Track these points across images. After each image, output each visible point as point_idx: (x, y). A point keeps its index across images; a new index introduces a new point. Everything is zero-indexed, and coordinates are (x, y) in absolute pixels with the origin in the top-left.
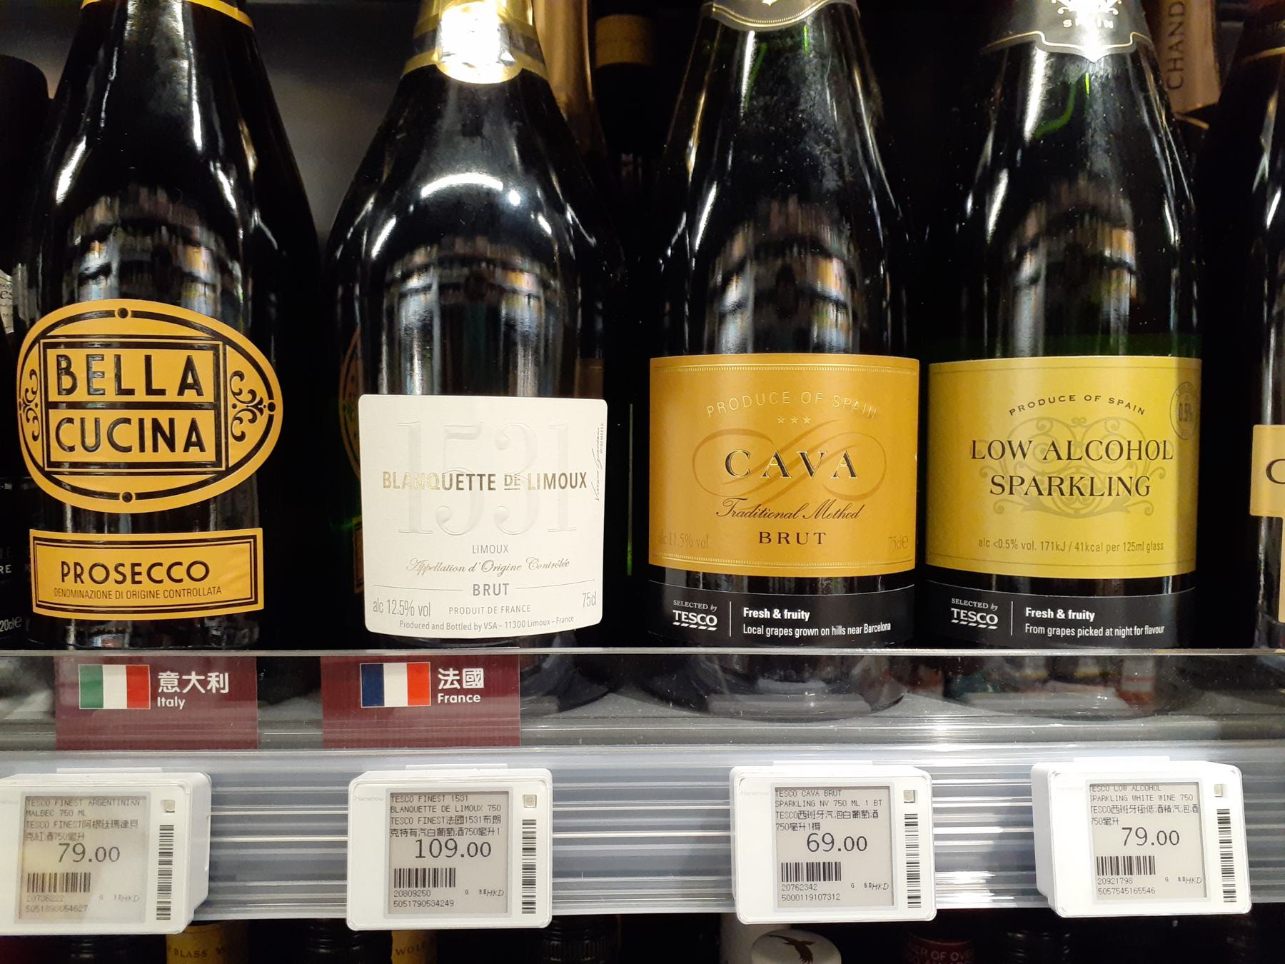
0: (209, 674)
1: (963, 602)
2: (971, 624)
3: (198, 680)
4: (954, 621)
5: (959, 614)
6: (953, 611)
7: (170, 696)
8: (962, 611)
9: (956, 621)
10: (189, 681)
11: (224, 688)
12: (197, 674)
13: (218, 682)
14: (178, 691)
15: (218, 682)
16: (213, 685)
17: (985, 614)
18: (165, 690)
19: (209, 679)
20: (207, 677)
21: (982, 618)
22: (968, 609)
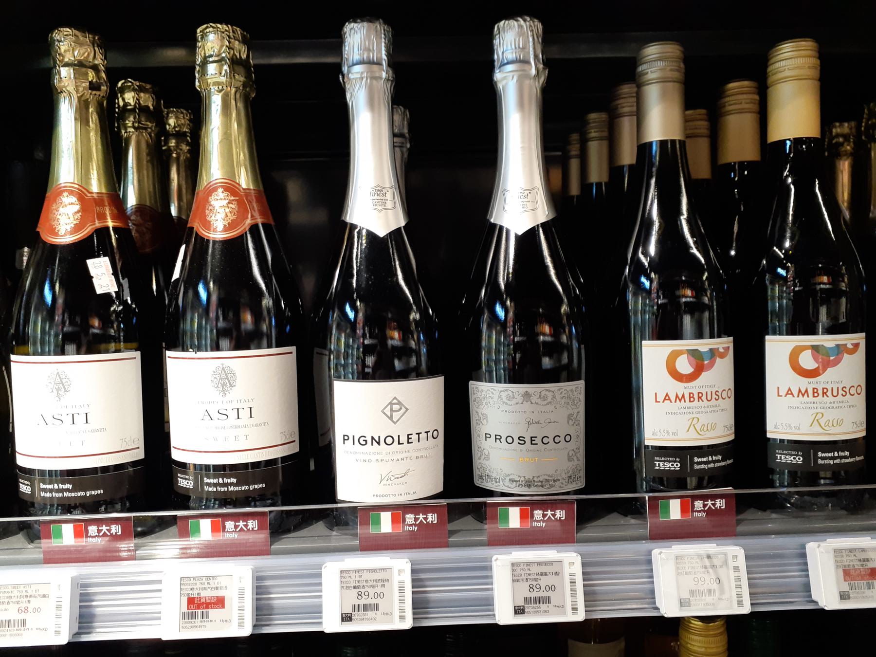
0: (556, 511)
1: (783, 451)
2: (788, 462)
3: (552, 514)
4: (777, 461)
5: (781, 457)
6: (777, 456)
7: (538, 521)
8: (783, 456)
9: (779, 461)
10: (547, 514)
11: (563, 517)
12: (551, 511)
13: (560, 514)
14: (542, 519)
15: (560, 514)
16: (558, 516)
17: (795, 457)
18: (537, 519)
19: (556, 513)
20: (555, 512)
21: (794, 458)
22: (786, 455)
